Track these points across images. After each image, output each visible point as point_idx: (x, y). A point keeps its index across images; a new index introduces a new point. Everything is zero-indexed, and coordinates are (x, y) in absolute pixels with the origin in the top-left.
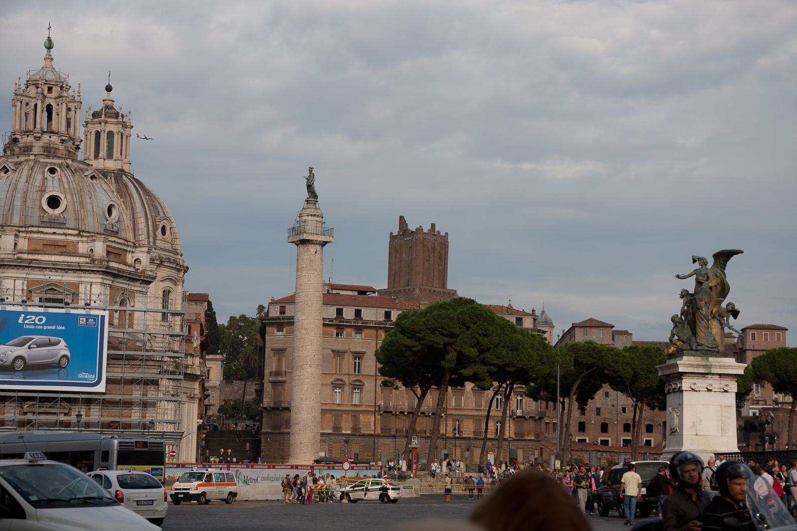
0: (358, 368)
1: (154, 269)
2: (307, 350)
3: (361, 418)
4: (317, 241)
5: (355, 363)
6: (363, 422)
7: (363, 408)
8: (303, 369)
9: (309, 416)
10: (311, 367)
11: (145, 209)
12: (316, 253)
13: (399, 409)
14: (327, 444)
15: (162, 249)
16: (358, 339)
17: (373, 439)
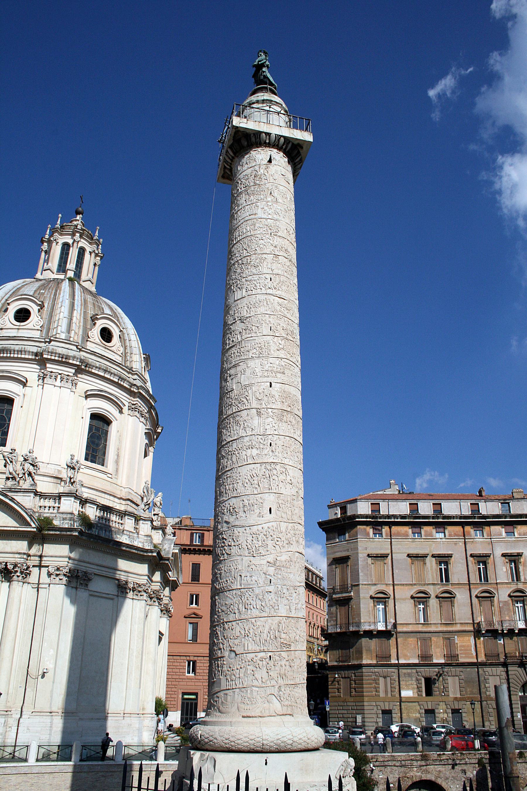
0: (445, 576)
1: (72, 375)
2: (248, 372)
3: (456, 642)
4: (268, 134)
5: (441, 569)
6: (461, 646)
7: (458, 628)
8: (237, 423)
9: (256, 561)
10: (259, 414)
11: (74, 299)
12: (270, 161)
13: (506, 626)
14: (414, 679)
15: (94, 353)
16: (441, 539)
17: (476, 669)
